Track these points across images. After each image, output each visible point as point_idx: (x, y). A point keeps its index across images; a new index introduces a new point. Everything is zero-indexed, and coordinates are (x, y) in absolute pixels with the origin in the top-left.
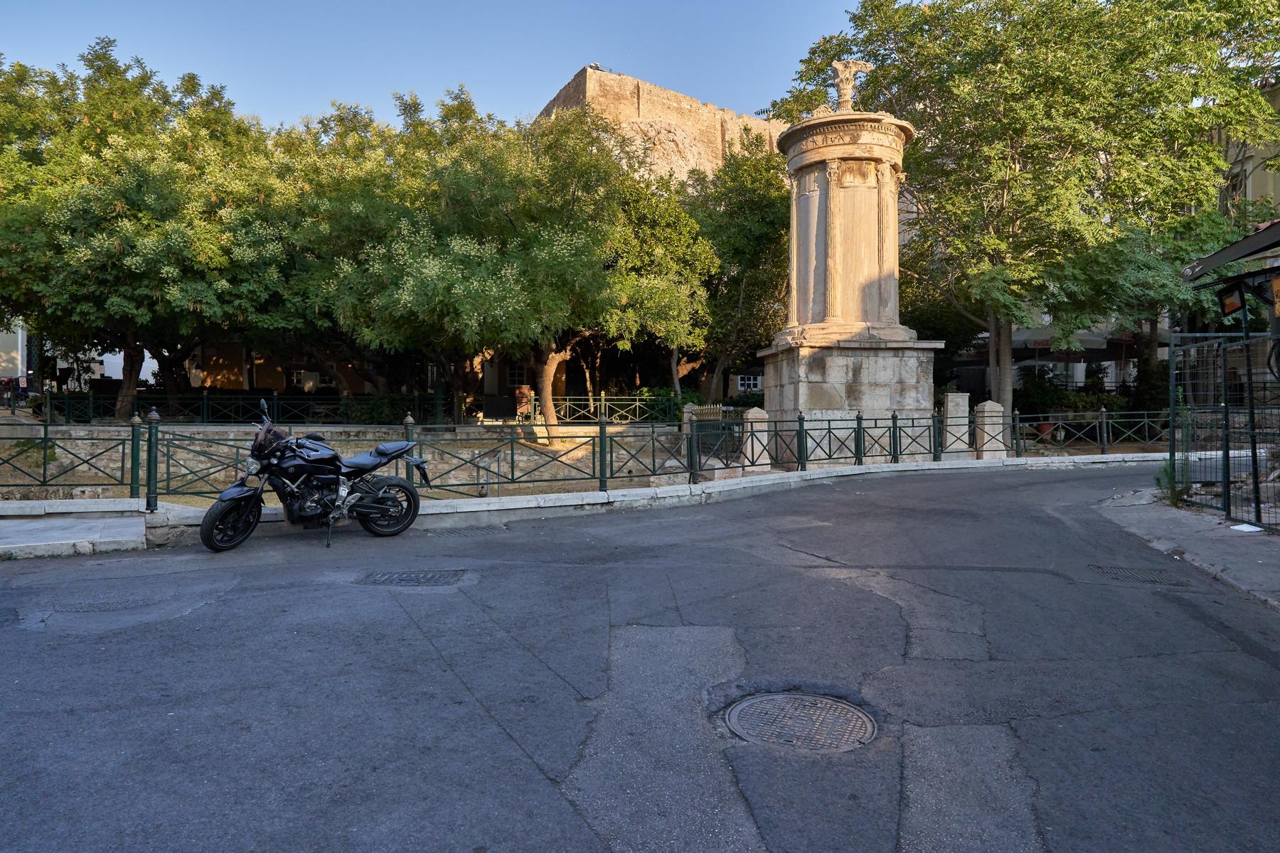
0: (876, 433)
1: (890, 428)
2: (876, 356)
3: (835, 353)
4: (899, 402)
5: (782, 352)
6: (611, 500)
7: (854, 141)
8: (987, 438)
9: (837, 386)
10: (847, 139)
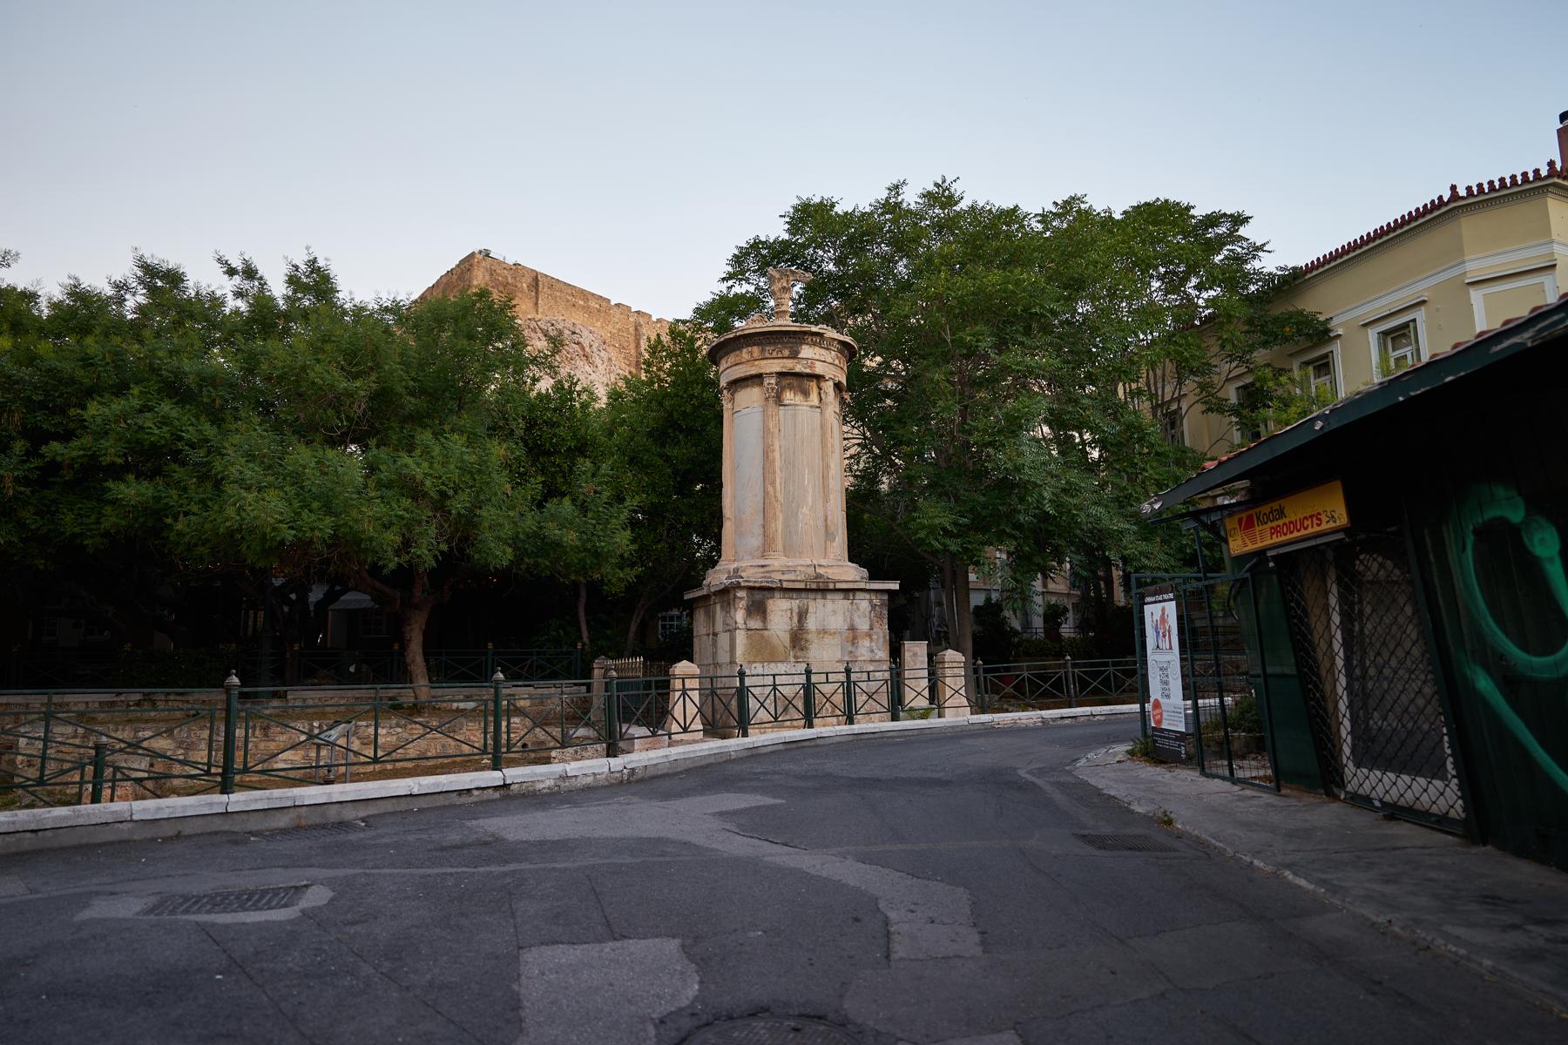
0: (827, 689)
1: (843, 683)
2: (824, 598)
3: (777, 594)
4: (851, 652)
5: (716, 593)
6: (508, 782)
7: (794, 355)
8: (948, 692)
9: (781, 634)
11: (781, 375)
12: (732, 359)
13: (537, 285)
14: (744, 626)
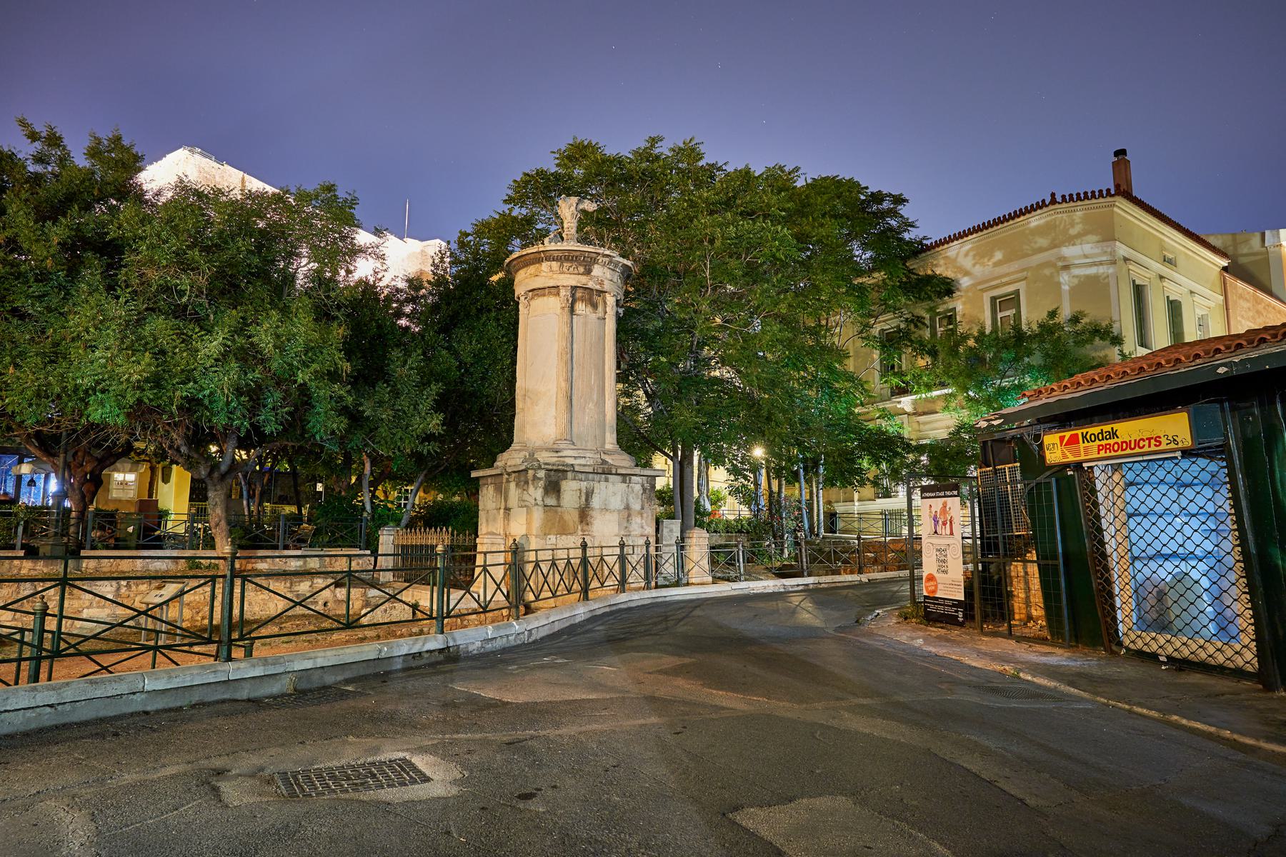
2: (607, 480)
7: (588, 272)
10: (581, 269)
11: (574, 288)
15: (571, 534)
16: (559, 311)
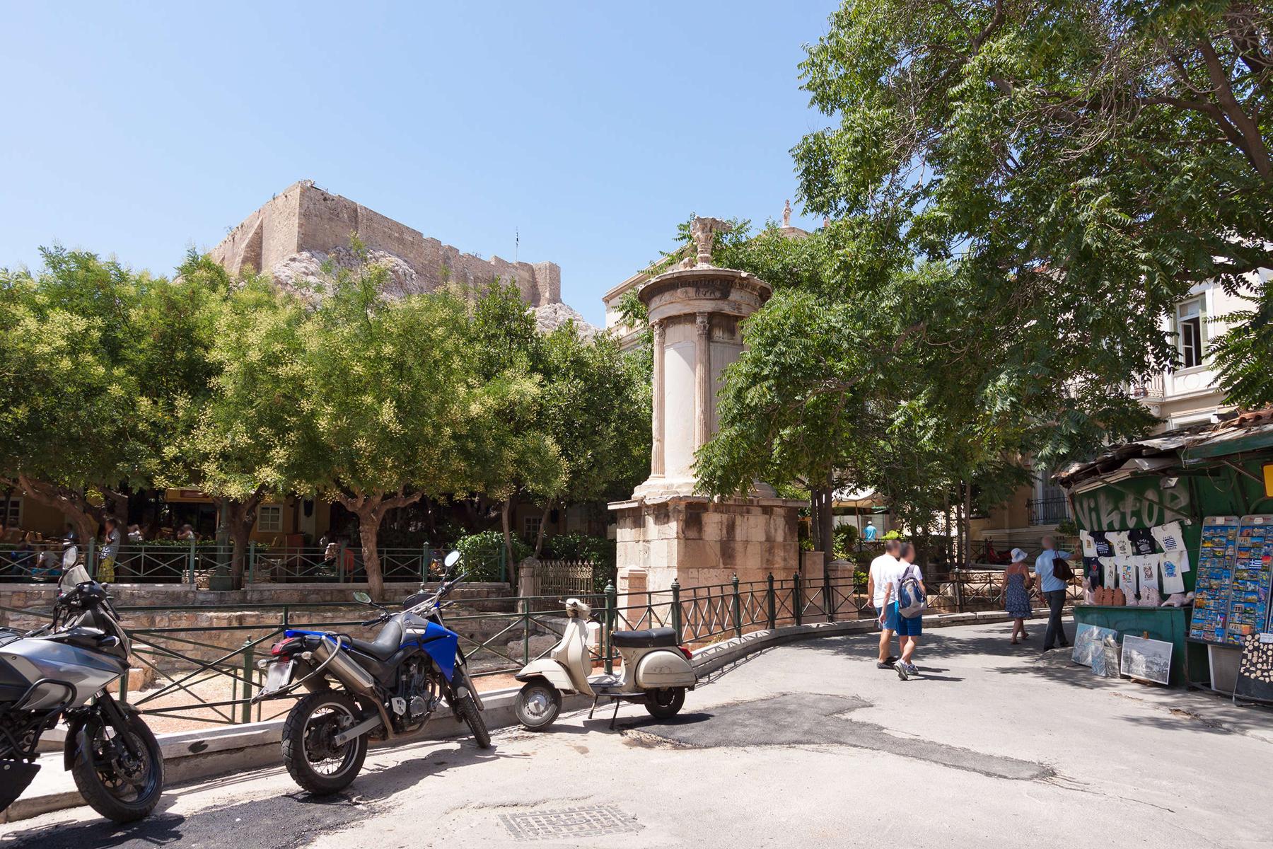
2: (748, 512)
7: (725, 296)
8: (841, 599)
10: (718, 295)
11: (711, 316)
12: (667, 297)
13: (357, 216)
14: (681, 536)
15: (713, 567)
16: (696, 338)
